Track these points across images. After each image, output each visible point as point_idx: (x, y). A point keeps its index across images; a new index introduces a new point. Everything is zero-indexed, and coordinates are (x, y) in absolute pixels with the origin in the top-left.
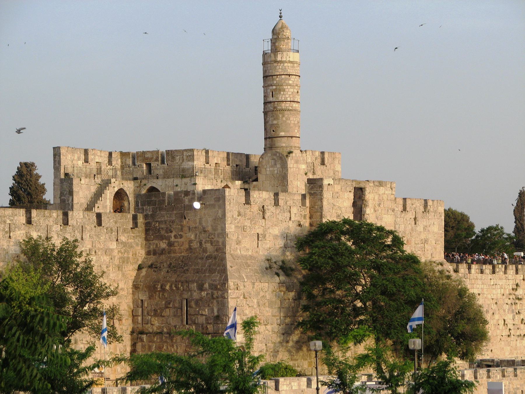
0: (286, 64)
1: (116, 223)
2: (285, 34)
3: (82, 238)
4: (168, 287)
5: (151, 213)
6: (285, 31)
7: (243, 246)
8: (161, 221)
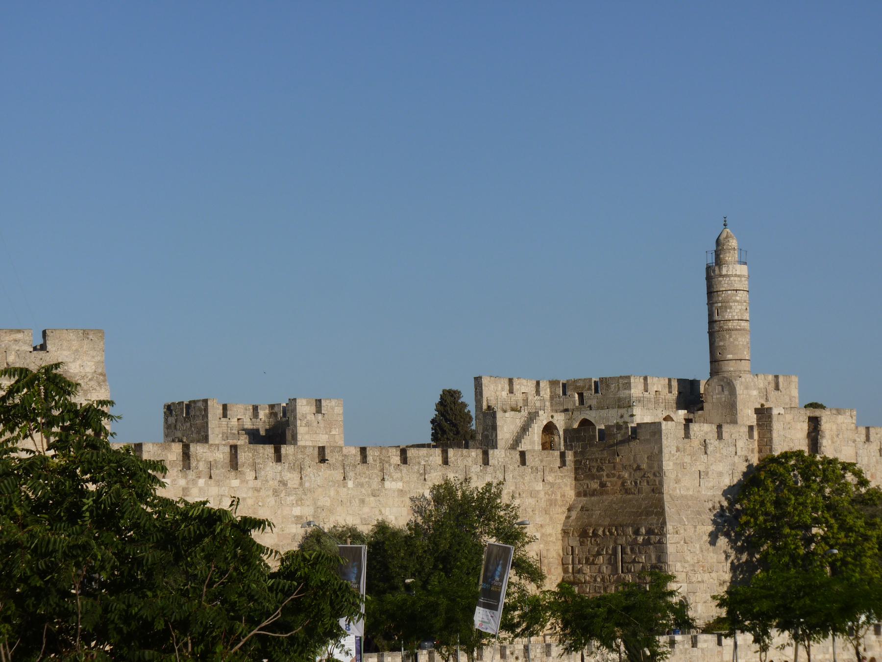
0: (732, 278)
1: (542, 461)
2: (730, 244)
3: (504, 479)
4: (600, 532)
6: (731, 241)
7: (683, 485)
8: (592, 459)
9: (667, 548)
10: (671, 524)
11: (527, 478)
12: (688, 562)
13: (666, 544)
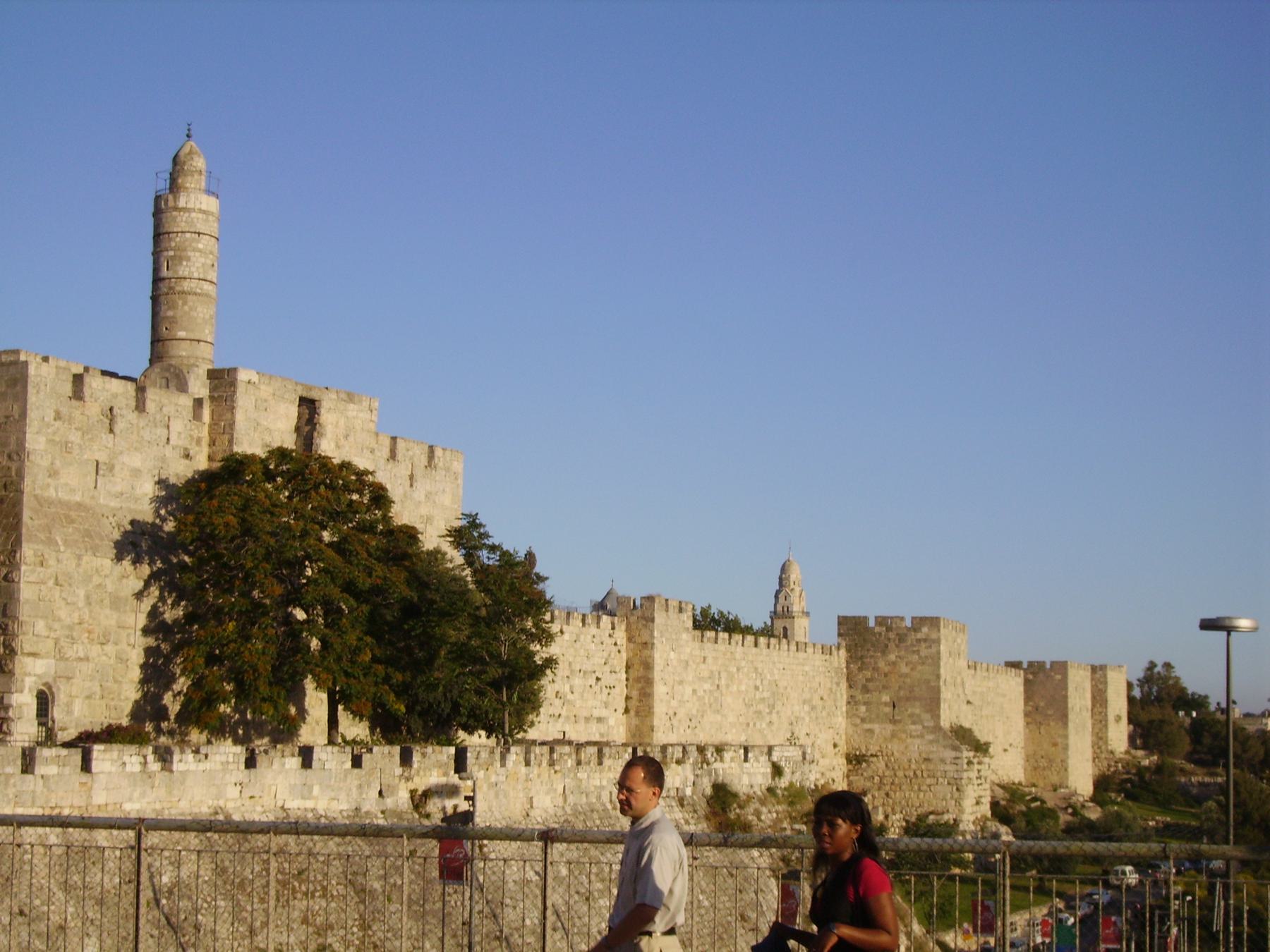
0: (193, 215)
2: (194, 164)
6: (196, 158)
7: (62, 481)
9: (19, 589)
10: (31, 546)
12: (59, 620)
13: (19, 582)
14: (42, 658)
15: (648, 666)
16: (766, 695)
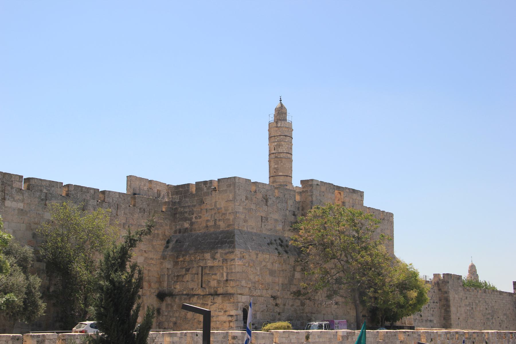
0: (283, 129)
1: (148, 205)
2: (283, 111)
3: (117, 215)
5: (178, 200)
8: (186, 206)
10: (239, 250)
11: (136, 216)
14: (244, 295)
15: (447, 300)
16: (490, 312)
